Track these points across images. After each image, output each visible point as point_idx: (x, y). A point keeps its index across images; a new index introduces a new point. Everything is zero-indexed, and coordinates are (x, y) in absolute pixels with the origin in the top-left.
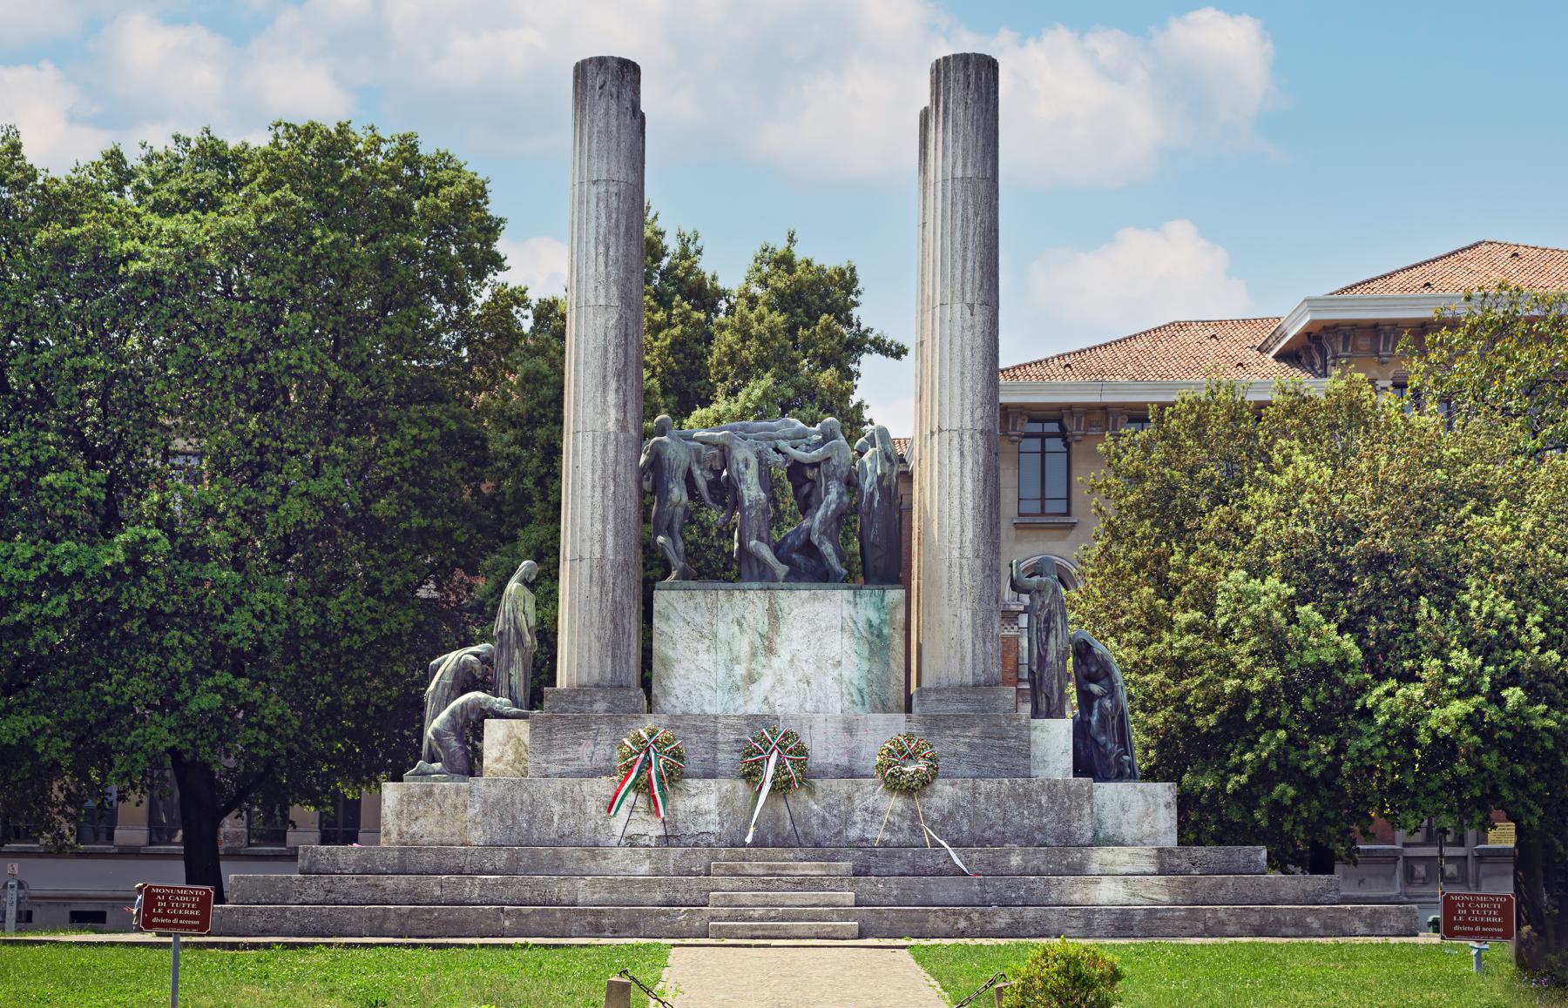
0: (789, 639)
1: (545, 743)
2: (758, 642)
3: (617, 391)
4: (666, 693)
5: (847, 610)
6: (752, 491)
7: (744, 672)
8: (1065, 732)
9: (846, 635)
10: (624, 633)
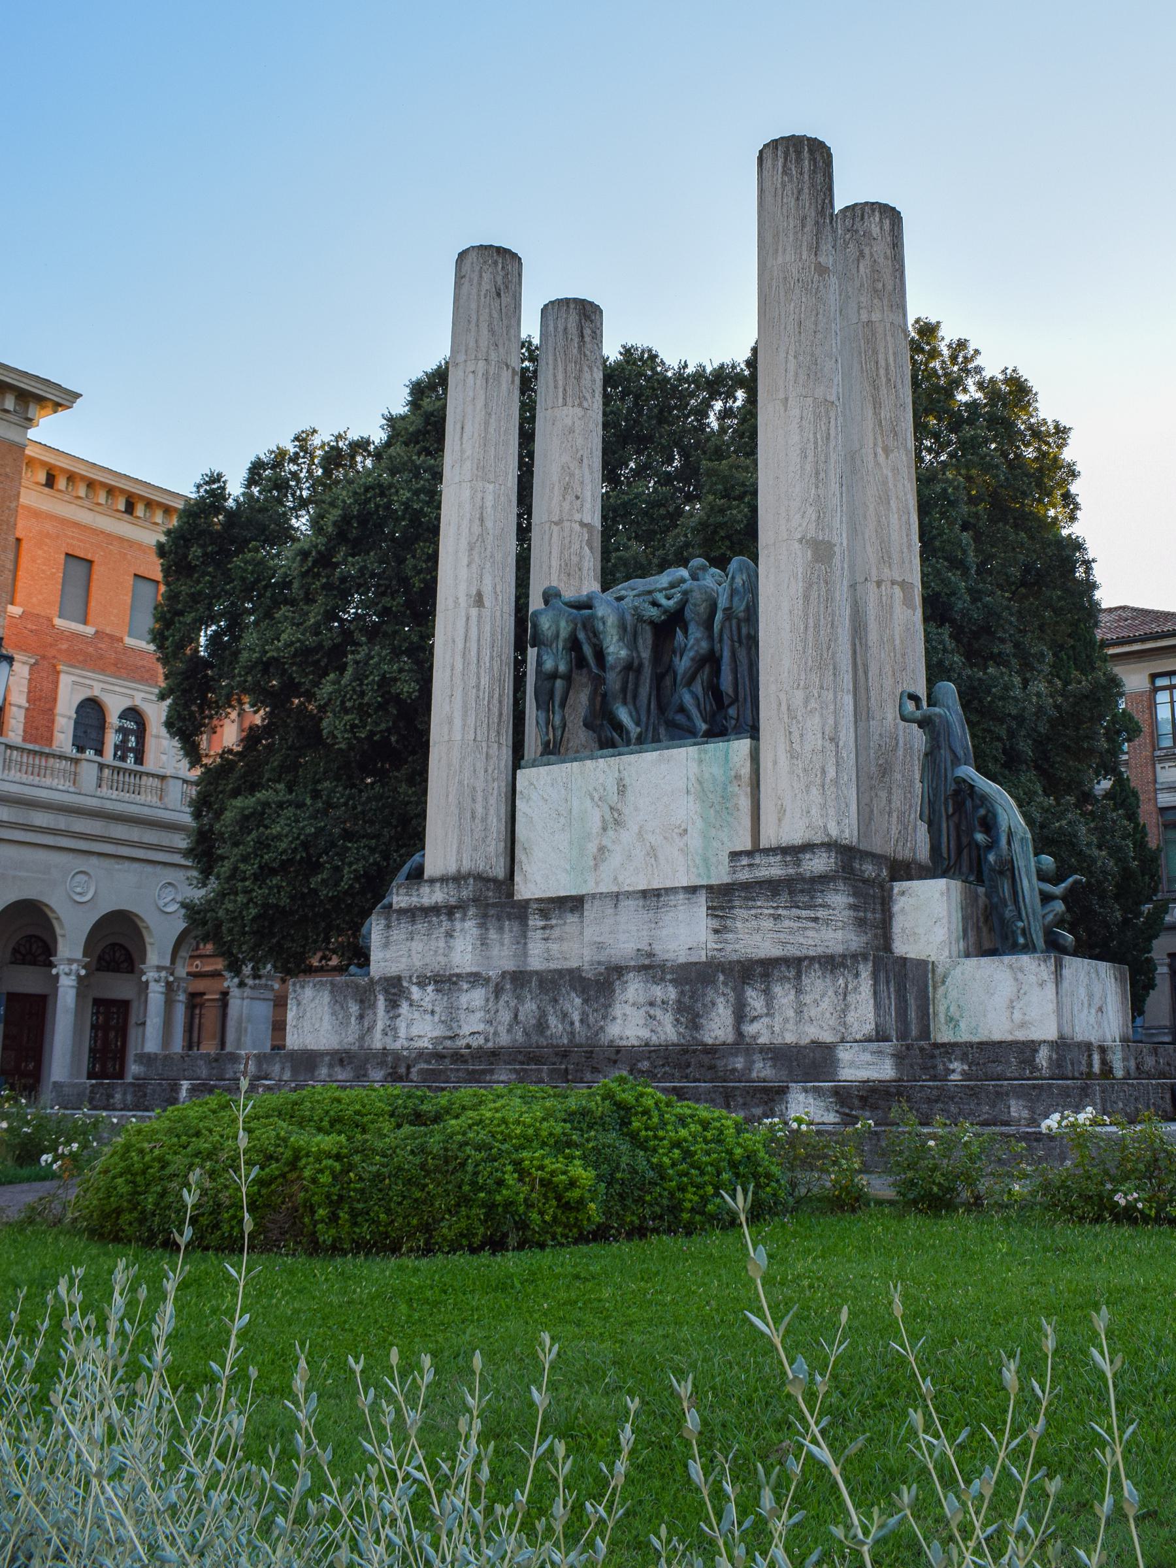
0: (636, 809)
1: (384, 941)
2: (608, 817)
4: (525, 881)
5: (694, 768)
6: (616, 650)
7: (595, 850)
8: (937, 895)
9: (691, 798)
10: (473, 817)
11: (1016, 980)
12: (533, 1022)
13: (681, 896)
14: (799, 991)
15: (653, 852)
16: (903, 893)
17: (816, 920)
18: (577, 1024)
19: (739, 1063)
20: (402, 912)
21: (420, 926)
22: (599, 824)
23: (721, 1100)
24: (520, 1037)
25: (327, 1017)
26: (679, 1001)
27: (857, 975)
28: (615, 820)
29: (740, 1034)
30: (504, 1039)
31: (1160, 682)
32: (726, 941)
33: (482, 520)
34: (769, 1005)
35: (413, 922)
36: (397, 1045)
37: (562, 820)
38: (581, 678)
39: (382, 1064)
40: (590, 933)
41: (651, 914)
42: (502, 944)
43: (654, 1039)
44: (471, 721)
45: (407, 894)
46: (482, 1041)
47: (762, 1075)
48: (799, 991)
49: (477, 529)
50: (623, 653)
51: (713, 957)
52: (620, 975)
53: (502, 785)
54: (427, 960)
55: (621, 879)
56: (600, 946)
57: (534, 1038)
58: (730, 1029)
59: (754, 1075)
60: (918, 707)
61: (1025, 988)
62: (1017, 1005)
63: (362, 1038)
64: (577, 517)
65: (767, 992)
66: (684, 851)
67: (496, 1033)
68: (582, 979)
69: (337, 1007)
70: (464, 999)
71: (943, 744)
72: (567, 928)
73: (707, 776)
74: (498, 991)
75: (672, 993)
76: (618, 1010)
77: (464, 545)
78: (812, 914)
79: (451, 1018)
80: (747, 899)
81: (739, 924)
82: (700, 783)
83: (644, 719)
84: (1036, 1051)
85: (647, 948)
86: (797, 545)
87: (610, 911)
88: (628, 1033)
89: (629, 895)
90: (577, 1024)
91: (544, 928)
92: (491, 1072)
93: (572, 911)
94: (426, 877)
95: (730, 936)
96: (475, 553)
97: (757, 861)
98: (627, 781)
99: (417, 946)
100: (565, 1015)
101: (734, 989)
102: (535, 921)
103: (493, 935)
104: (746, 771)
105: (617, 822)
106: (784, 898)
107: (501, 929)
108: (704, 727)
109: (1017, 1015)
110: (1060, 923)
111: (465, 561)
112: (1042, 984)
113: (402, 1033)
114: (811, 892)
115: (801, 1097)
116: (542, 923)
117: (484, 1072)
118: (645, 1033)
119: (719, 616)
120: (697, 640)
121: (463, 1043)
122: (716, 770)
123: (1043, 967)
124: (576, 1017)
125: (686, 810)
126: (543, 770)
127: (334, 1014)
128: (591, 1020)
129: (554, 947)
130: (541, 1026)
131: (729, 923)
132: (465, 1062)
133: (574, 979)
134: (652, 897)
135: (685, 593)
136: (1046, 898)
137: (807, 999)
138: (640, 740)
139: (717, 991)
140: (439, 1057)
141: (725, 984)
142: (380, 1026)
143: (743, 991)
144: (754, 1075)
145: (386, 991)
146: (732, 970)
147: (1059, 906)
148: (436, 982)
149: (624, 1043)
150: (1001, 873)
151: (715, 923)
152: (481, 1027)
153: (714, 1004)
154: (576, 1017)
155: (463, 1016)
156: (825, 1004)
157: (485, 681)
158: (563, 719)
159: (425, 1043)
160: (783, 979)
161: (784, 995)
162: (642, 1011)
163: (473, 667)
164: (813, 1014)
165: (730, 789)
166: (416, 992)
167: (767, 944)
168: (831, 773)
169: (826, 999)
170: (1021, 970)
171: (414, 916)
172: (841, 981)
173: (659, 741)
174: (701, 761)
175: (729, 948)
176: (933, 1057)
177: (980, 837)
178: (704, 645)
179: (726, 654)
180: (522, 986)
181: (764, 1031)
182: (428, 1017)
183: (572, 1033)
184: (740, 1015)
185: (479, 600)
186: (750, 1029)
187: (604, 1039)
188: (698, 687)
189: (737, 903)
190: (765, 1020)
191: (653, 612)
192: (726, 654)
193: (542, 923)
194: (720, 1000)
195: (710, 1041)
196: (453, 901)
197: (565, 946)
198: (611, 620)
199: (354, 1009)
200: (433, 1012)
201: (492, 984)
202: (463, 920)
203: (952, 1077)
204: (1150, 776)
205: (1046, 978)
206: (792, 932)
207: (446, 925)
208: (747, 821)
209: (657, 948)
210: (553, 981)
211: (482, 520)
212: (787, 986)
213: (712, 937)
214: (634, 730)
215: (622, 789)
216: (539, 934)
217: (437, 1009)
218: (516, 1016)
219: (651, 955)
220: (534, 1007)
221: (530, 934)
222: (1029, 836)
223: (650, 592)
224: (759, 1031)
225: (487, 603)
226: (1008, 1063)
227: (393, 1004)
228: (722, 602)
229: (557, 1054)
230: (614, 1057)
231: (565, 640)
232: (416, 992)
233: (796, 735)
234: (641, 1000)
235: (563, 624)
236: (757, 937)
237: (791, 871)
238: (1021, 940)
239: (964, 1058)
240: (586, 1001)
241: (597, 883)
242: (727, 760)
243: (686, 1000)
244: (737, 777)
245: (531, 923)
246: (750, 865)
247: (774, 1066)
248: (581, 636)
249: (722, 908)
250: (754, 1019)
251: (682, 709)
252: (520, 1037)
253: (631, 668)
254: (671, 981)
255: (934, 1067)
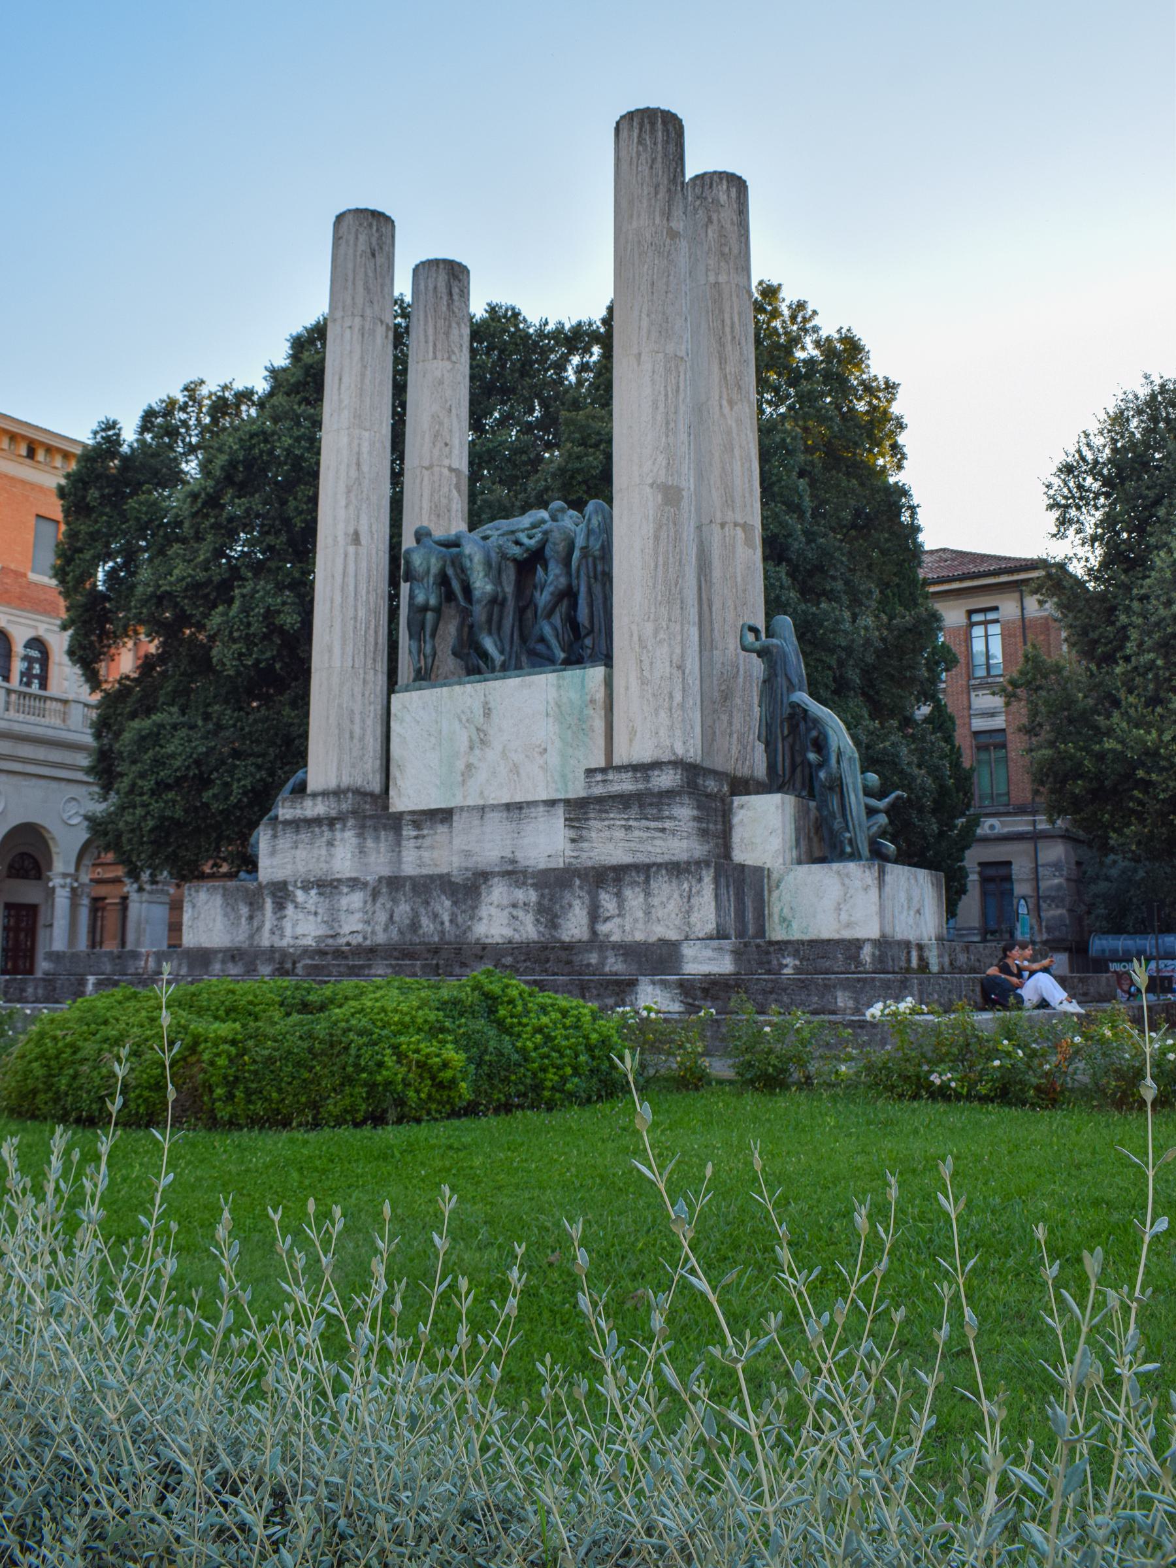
0: (500, 730)
2: (475, 737)
3: (347, 506)
4: (400, 795)
5: (553, 694)
6: (482, 585)
8: (773, 809)
9: (551, 720)
10: (352, 737)
11: (843, 884)
12: (408, 922)
13: (541, 809)
14: (648, 894)
15: (515, 769)
16: (742, 807)
17: (663, 830)
18: (447, 924)
19: (593, 958)
20: (287, 823)
21: (304, 836)
22: (466, 744)
23: (576, 991)
24: (394, 935)
25: (219, 918)
26: (539, 903)
27: (700, 880)
28: (481, 739)
29: (594, 933)
30: (381, 938)
31: (977, 618)
32: (581, 850)
33: (358, 464)
34: (620, 906)
35: (297, 832)
36: (284, 943)
37: (433, 740)
38: (450, 611)
39: (271, 960)
40: (459, 842)
41: (514, 825)
42: (379, 852)
43: (517, 938)
44: (349, 649)
45: (292, 807)
46: (360, 939)
47: (614, 969)
48: (648, 894)
49: (353, 473)
50: (489, 588)
51: (570, 864)
52: (486, 880)
53: (378, 708)
54: (311, 867)
55: (486, 793)
56: (468, 854)
57: (408, 937)
58: (585, 928)
59: (607, 969)
60: (757, 638)
61: (851, 891)
62: (844, 907)
63: (251, 937)
64: (446, 462)
65: (618, 895)
66: (544, 768)
67: (373, 933)
68: (451, 883)
69: (229, 909)
70: (344, 902)
71: (779, 671)
72: (437, 837)
73: (565, 700)
74: (375, 895)
75: (533, 896)
76: (484, 911)
77: (342, 488)
78: (659, 825)
79: (333, 919)
80: (601, 811)
81: (593, 834)
82: (559, 707)
83: (507, 648)
84: (861, 948)
85: (510, 855)
86: (648, 490)
87: (476, 822)
88: (493, 931)
89: (494, 807)
90: (447, 924)
91: (416, 837)
92: (369, 967)
93: (442, 821)
94: (309, 790)
95: (585, 845)
96: (352, 495)
97: (610, 777)
98: (492, 705)
99: (301, 853)
100: (436, 916)
101: (589, 893)
102: (408, 832)
103: (370, 843)
104: (600, 695)
105: (482, 742)
106: (634, 811)
107: (377, 839)
108: (562, 655)
109: (844, 917)
110: (883, 834)
111: (343, 503)
112: (866, 889)
113: (288, 932)
114: (659, 805)
115: (650, 989)
116: (415, 833)
117: (362, 967)
118: (508, 932)
119: (576, 554)
120: (557, 576)
121: (343, 941)
122: (574, 695)
123: (868, 873)
124: (446, 918)
125: (546, 731)
126: (415, 694)
127: (226, 915)
128: (460, 920)
129: (426, 854)
130: (415, 926)
131: (584, 833)
132: (346, 958)
133: (444, 883)
134: (514, 809)
135: (546, 533)
136: (871, 812)
137: (655, 901)
138: (504, 667)
139: (573, 894)
140: (322, 953)
141: (581, 888)
142: (268, 926)
143: (597, 895)
144: (607, 969)
145: (273, 895)
146: (586, 875)
147: (883, 819)
148: (319, 886)
149: (489, 941)
150: (831, 788)
151: (572, 834)
152: (359, 927)
153: (570, 906)
154: (446, 918)
155: (343, 916)
156: (671, 906)
157: (362, 613)
158: (434, 647)
159: (309, 942)
160: (634, 883)
161: (634, 898)
162: (506, 912)
163: (351, 600)
164: (660, 914)
165: (586, 712)
166: (300, 896)
167: (619, 852)
168: (678, 697)
169: (672, 902)
170: (848, 875)
171: (298, 827)
172: (686, 886)
173: (521, 668)
174: (559, 687)
175: (585, 855)
176: (768, 953)
177: (812, 756)
178: (563, 581)
179: (583, 589)
180: (397, 890)
181: (616, 930)
182: (311, 918)
183: (443, 932)
184: (594, 916)
185: (356, 539)
186: (603, 928)
187: (471, 938)
188: (557, 619)
189: (592, 815)
190: (617, 920)
191: (516, 550)
192: (583, 589)
193: (415, 833)
194: (577, 903)
195: (567, 939)
196: (333, 813)
197: (436, 854)
198: (478, 558)
199: (244, 910)
200: (316, 914)
201: (369, 888)
202: (343, 830)
203: (785, 971)
204: (965, 703)
205: (870, 882)
206: (641, 841)
207: (327, 835)
208: (601, 742)
209: (519, 856)
210: (425, 885)
211: (358, 464)
212: (637, 889)
213: (569, 846)
214: (498, 658)
215: (487, 712)
216: (412, 843)
217: (320, 911)
218: (391, 917)
219: (514, 862)
220: (408, 908)
221: (404, 843)
222: (856, 755)
223: (513, 532)
224: (612, 930)
225: (363, 541)
226: (835, 958)
227: (280, 907)
228: (580, 542)
229: (429, 951)
230: (480, 953)
231: (435, 576)
232: (300, 896)
233: (646, 665)
234: (505, 902)
235: (433, 561)
236: (611, 846)
237: (641, 786)
238: (848, 849)
239: (796, 954)
240: (455, 903)
241: (465, 797)
242: (583, 686)
243: (546, 902)
244: (592, 701)
245: (404, 833)
246: (604, 781)
247: (625, 961)
248: (450, 572)
249: (578, 820)
250: (607, 919)
251: (542, 639)
252: (394, 935)
253: (496, 601)
254: (532, 885)
255: (769, 962)
